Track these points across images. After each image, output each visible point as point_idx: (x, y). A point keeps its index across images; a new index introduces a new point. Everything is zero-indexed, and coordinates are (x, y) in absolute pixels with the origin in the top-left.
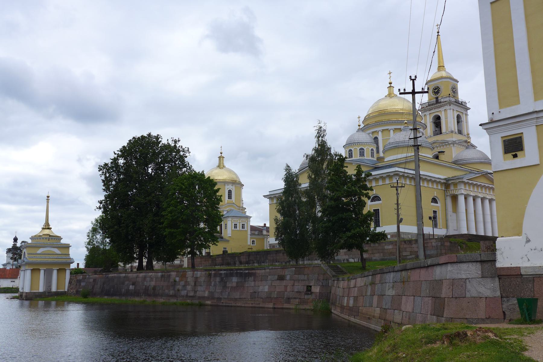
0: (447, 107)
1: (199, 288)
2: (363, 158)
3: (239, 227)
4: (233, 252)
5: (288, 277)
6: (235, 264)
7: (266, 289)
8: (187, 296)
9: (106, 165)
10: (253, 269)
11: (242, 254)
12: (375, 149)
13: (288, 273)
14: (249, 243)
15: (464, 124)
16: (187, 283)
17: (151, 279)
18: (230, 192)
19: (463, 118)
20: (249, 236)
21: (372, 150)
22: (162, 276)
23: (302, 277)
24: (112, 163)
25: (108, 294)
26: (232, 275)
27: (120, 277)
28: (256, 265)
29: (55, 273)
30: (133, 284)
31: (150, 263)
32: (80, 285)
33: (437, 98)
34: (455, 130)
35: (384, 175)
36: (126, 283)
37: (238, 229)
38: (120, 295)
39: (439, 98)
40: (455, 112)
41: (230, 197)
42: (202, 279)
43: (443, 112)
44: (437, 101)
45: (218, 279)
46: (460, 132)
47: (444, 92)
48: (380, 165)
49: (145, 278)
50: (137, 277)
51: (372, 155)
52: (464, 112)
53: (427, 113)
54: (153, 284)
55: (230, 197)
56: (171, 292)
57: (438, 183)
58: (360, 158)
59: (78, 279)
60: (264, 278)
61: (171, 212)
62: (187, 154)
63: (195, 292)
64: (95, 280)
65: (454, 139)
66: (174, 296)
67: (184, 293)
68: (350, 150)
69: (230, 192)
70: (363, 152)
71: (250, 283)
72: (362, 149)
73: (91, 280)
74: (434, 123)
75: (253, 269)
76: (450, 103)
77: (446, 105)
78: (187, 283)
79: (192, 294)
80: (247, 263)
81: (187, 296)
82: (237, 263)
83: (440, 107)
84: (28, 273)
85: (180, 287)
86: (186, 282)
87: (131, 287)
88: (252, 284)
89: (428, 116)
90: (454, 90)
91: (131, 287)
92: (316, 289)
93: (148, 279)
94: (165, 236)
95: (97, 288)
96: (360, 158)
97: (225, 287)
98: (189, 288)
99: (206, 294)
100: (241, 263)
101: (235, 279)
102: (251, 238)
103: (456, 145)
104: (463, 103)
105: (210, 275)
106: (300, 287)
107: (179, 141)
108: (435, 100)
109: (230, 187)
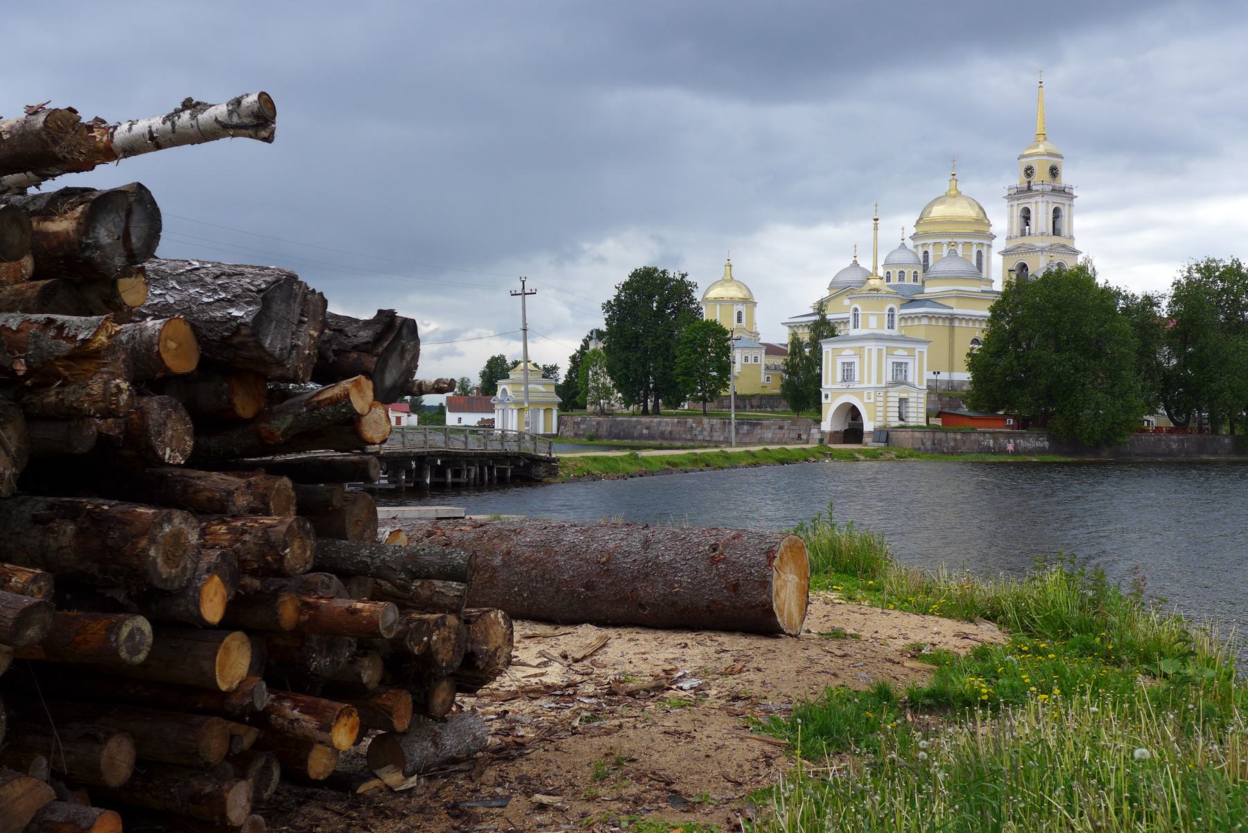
0: (1039, 199)
1: (715, 434)
2: (902, 283)
3: (751, 361)
4: (743, 393)
5: (786, 427)
6: (745, 407)
7: (770, 435)
8: (704, 440)
9: (609, 302)
10: (760, 420)
11: (753, 396)
12: (920, 272)
13: (786, 424)
14: (762, 381)
15: (1064, 221)
16: (703, 429)
17: (667, 424)
18: (739, 313)
19: (1065, 211)
20: (763, 371)
21: (915, 272)
22: (678, 422)
23: (795, 427)
24: (615, 300)
25: (617, 437)
27: (631, 421)
28: (769, 409)
29: (542, 412)
30: (646, 429)
31: (656, 405)
32: (579, 427)
33: (1029, 182)
34: (1047, 229)
35: (913, 316)
36: (639, 427)
37: (749, 362)
38: (633, 438)
39: (1032, 184)
41: (739, 320)
42: (718, 426)
43: (1034, 205)
44: (1029, 189)
46: (1056, 232)
47: (1041, 174)
48: (918, 297)
49: (660, 423)
50: (651, 422)
51: (915, 279)
52: (1067, 203)
53: (1015, 203)
54: (669, 429)
55: (739, 320)
56: (689, 437)
57: (981, 322)
58: (900, 283)
59: (576, 420)
60: (768, 427)
61: (684, 361)
62: (695, 290)
63: (712, 437)
64: (598, 423)
65: (1044, 245)
66: (692, 440)
67: (700, 437)
68: (888, 273)
69: (739, 313)
70: (904, 276)
71: (758, 431)
72: (902, 272)
73: (595, 423)
74: (1024, 217)
75: (760, 420)
76: (1043, 193)
77: (1037, 195)
78: (703, 429)
79: (708, 438)
80: (759, 407)
81: (704, 440)
82: (748, 406)
83: (1031, 197)
84: (515, 412)
85: (697, 433)
86: (703, 428)
87: (645, 431)
88: (760, 431)
89: (1015, 207)
90: (1054, 172)
91: (645, 431)
93: (664, 424)
94: (679, 383)
95: (603, 431)
96: (900, 283)
98: (705, 433)
99: (722, 439)
100: (752, 407)
101: (746, 427)
102: (765, 374)
103: (1045, 253)
104: (1067, 190)
105: (725, 423)
107: (686, 275)
108: (1026, 185)
109: (740, 307)
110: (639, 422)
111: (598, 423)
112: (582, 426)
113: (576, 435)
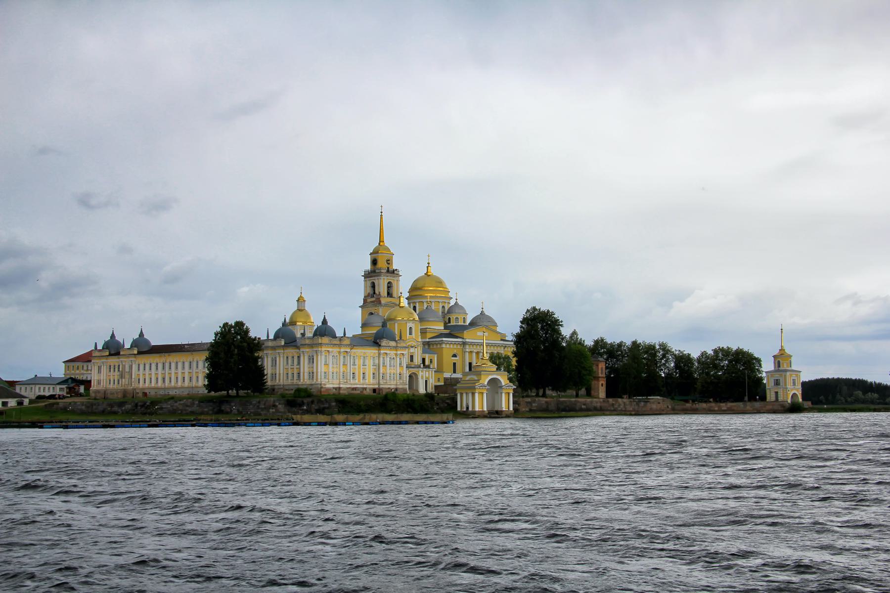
16: (619, 405)
17: (597, 402)
26: (641, 401)
30: (584, 405)
32: (532, 405)
36: (578, 404)
40: (385, 280)
45: (635, 403)
47: (381, 264)
56: (612, 409)
67: (619, 409)
78: (619, 405)
91: (583, 407)
92: (670, 407)
97: (639, 406)
98: (621, 407)
99: (631, 409)
106: (665, 406)
110: (578, 402)
111: (546, 402)
112: (534, 405)
113: (531, 411)
